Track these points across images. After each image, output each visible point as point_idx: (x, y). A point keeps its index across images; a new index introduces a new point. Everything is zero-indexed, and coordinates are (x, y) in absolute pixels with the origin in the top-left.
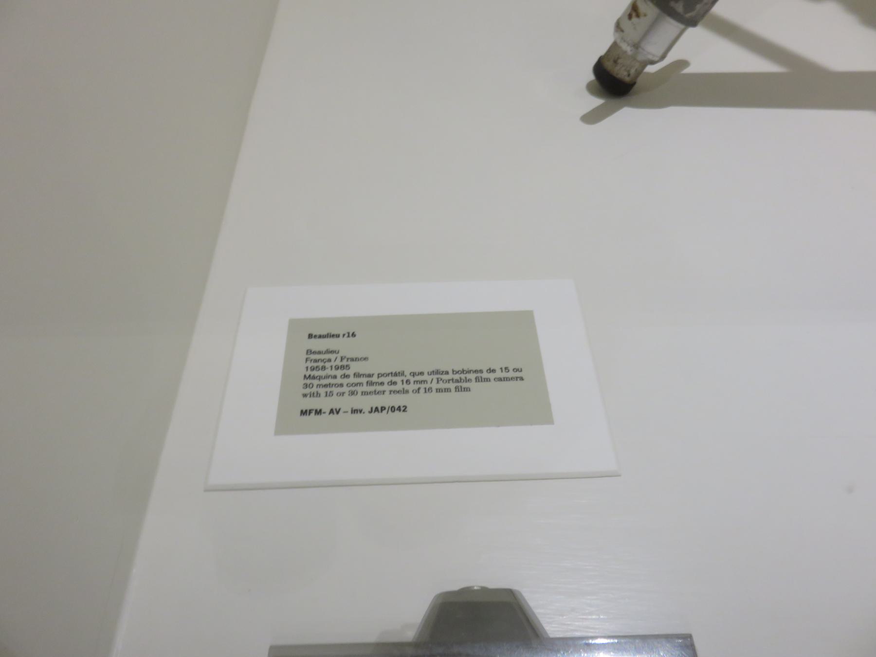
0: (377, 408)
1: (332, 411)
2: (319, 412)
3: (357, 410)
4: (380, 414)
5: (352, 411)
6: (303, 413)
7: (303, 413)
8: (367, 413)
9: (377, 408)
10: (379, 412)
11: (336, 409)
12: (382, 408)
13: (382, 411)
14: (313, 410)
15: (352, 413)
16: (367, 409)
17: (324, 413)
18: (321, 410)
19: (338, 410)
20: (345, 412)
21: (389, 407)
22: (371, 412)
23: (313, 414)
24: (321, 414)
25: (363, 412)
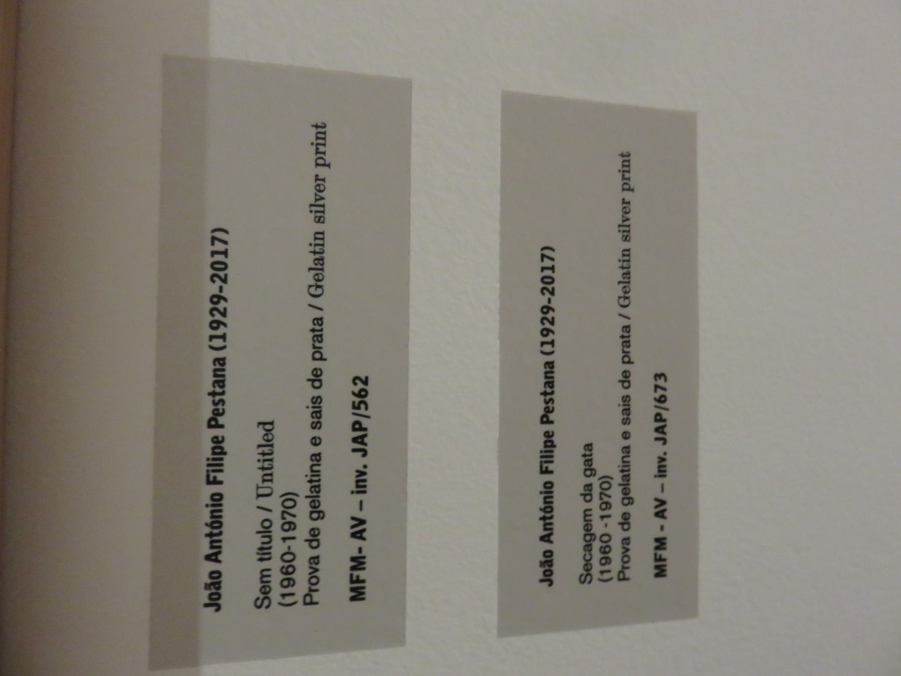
0: (355, 440)
1: (358, 535)
2: (358, 562)
3: (357, 481)
4: (368, 432)
5: (358, 492)
6: (358, 593)
7: (358, 593)
8: (365, 460)
9: (355, 440)
10: (365, 436)
11: (353, 527)
12: (354, 429)
13: (362, 429)
14: (351, 575)
15: (364, 492)
16: (358, 461)
17: (360, 550)
18: (353, 559)
19: (354, 522)
20: (361, 509)
21: (354, 414)
22: (365, 453)
23: (362, 575)
24: (364, 557)
25: (362, 469)
